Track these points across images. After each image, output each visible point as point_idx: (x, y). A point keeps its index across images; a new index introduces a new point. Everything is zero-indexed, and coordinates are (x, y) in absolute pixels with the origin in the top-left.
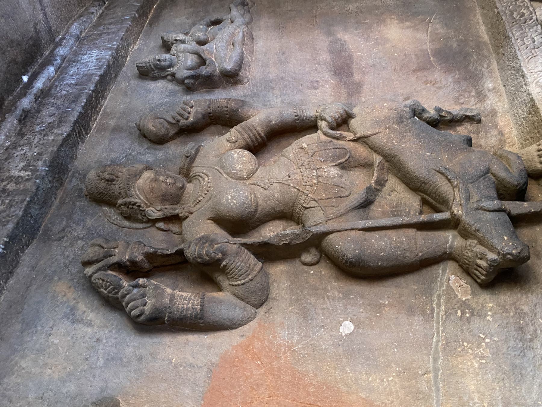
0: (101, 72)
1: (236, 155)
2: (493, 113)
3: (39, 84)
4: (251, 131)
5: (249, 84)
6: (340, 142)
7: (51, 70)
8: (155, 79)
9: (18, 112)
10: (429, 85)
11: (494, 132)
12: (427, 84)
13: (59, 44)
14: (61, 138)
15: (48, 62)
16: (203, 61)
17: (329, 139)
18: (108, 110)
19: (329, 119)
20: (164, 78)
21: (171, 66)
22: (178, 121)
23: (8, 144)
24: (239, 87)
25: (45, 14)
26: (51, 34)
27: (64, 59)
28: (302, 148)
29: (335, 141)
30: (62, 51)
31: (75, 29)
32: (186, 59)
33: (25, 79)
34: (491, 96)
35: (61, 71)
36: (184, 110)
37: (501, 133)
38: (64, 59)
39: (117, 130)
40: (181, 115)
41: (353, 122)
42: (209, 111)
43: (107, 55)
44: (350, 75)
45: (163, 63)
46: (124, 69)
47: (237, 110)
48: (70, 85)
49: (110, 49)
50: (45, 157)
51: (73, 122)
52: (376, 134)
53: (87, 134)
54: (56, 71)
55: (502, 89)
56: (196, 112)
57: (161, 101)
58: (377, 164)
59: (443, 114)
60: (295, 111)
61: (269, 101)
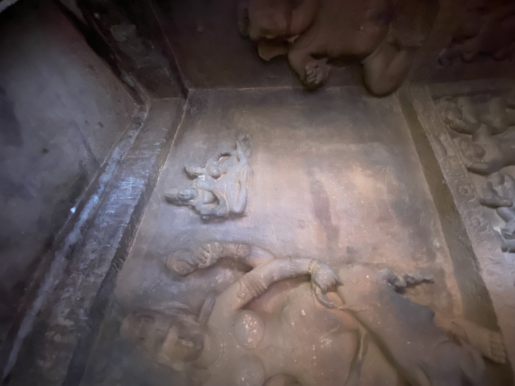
0: (135, 203)
1: (247, 326)
2: (442, 273)
3: (85, 216)
4: (258, 287)
5: (251, 217)
6: (332, 311)
7: (96, 199)
8: (179, 205)
9: (66, 248)
10: (389, 236)
11: (445, 294)
12: (388, 235)
13: (102, 171)
14: (100, 280)
15: (93, 191)
16: (216, 200)
17: (323, 307)
18: (142, 234)
19: (322, 287)
20: (186, 205)
21: (192, 198)
22: (198, 264)
23: (57, 282)
24: (244, 219)
25: (89, 150)
26: (96, 162)
27: (106, 185)
28: (301, 316)
29: (328, 310)
30: (105, 178)
31: (116, 154)
32: (203, 195)
33: (73, 210)
34: (439, 255)
35: (105, 197)
36: (203, 255)
37: (450, 295)
38: (106, 185)
39: (149, 256)
40: (201, 260)
41: (341, 288)
42: (222, 256)
43: (141, 183)
44: (329, 219)
45: (186, 197)
46: (155, 189)
47: (245, 258)
48: (111, 215)
49: (144, 177)
50: (87, 304)
51: (111, 260)
52: (363, 311)
53: (124, 260)
54: (100, 198)
55: (447, 249)
56: (212, 258)
57: (184, 229)
58: (363, 336)
59: (409, 280)
60: (293, 268)
61: (267, 236)
